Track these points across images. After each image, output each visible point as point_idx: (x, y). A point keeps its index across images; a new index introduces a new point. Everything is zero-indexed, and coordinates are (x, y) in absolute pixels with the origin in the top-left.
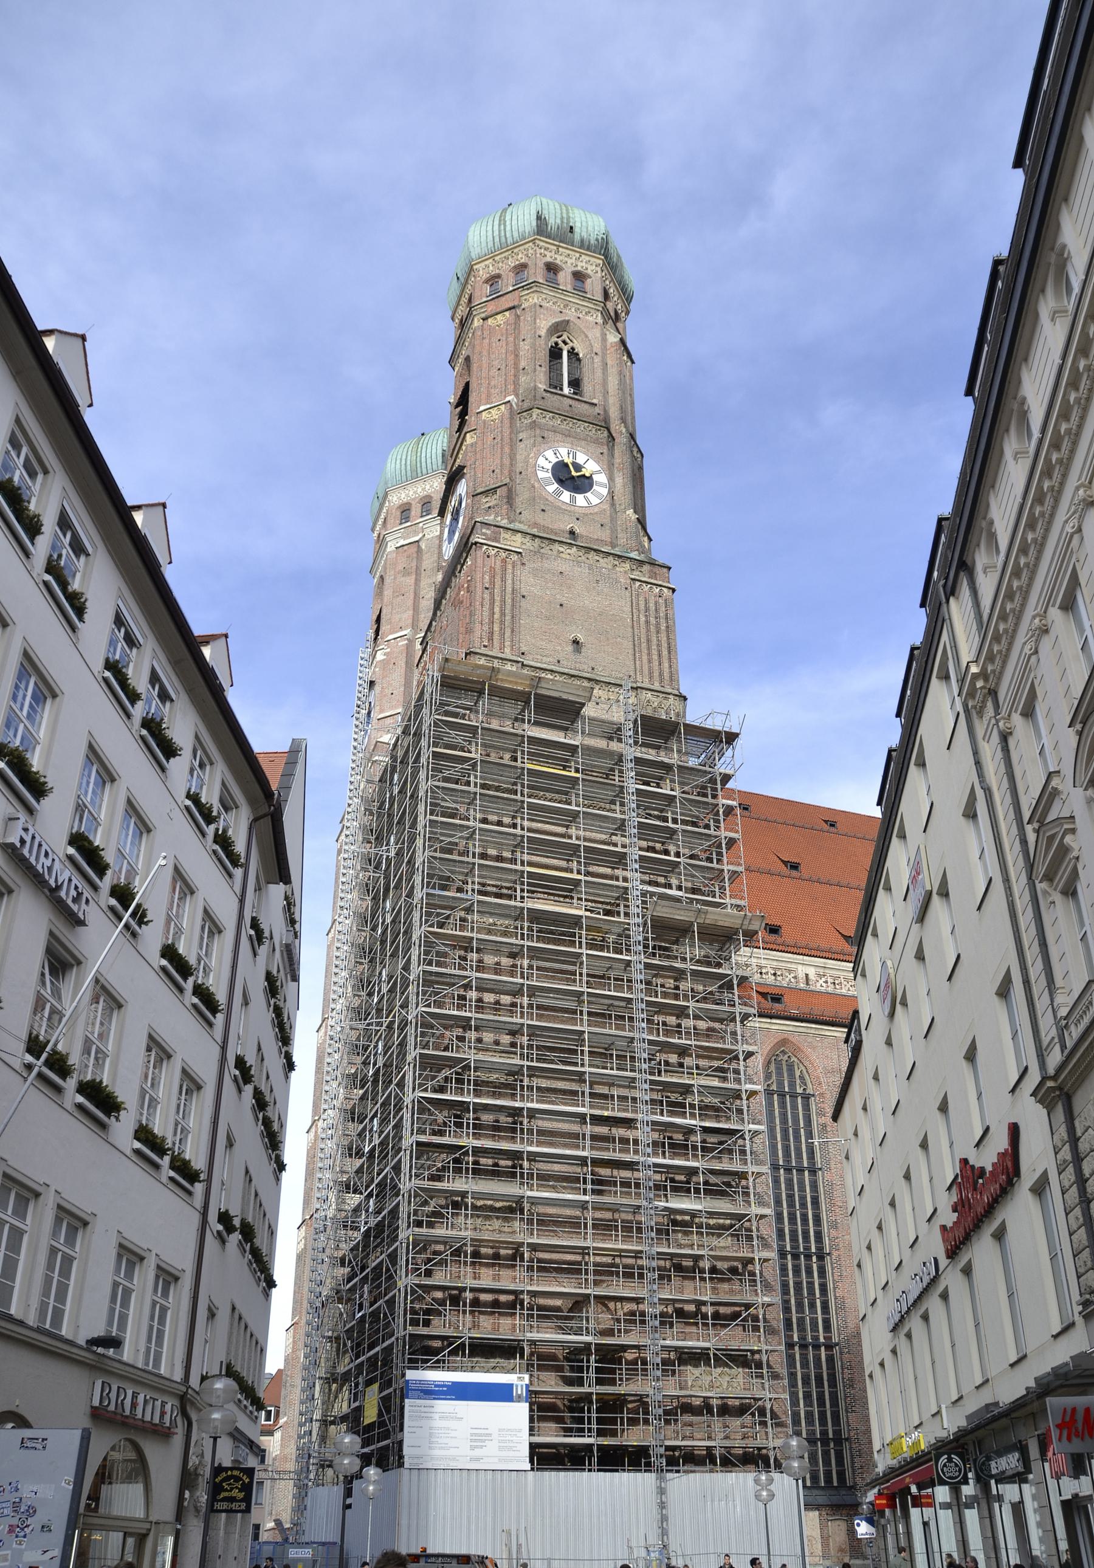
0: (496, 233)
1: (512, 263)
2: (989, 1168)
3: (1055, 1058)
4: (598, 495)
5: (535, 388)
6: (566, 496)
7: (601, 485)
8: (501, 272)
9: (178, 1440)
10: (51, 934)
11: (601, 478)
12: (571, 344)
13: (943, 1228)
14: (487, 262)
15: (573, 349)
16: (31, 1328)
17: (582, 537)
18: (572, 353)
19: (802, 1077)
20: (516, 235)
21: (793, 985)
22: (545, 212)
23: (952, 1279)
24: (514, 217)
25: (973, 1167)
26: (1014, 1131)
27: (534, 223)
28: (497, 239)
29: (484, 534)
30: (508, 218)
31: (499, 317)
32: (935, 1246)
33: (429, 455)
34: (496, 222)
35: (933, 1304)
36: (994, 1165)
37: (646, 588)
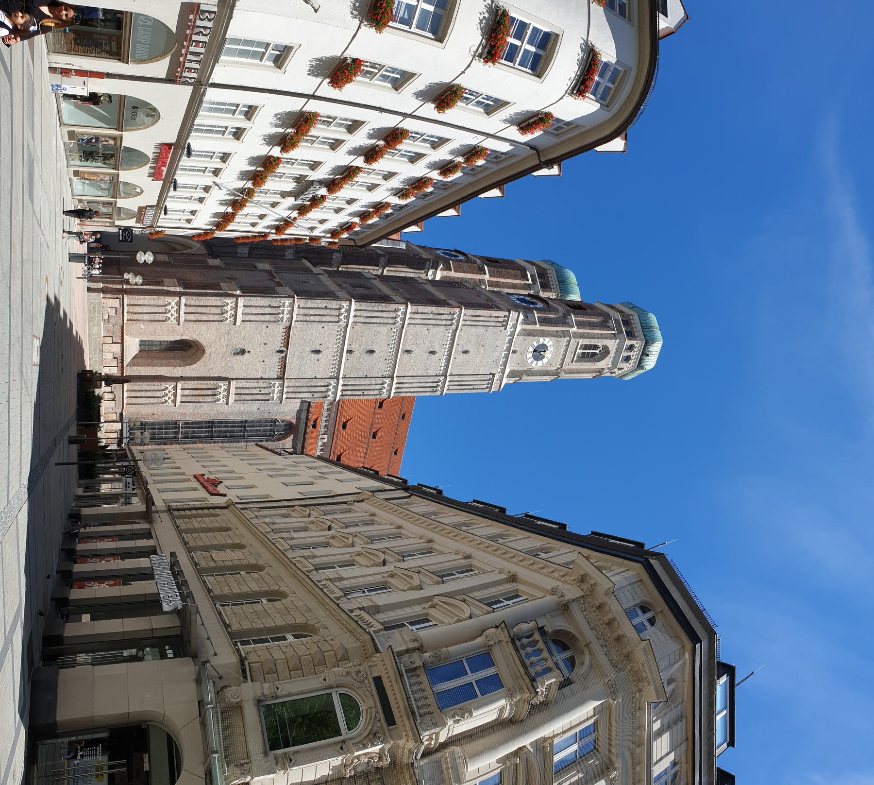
4: (532, 363)
7: (537, 364)
11: (540, 363)
25: (218, 484)
26: (225, 495)
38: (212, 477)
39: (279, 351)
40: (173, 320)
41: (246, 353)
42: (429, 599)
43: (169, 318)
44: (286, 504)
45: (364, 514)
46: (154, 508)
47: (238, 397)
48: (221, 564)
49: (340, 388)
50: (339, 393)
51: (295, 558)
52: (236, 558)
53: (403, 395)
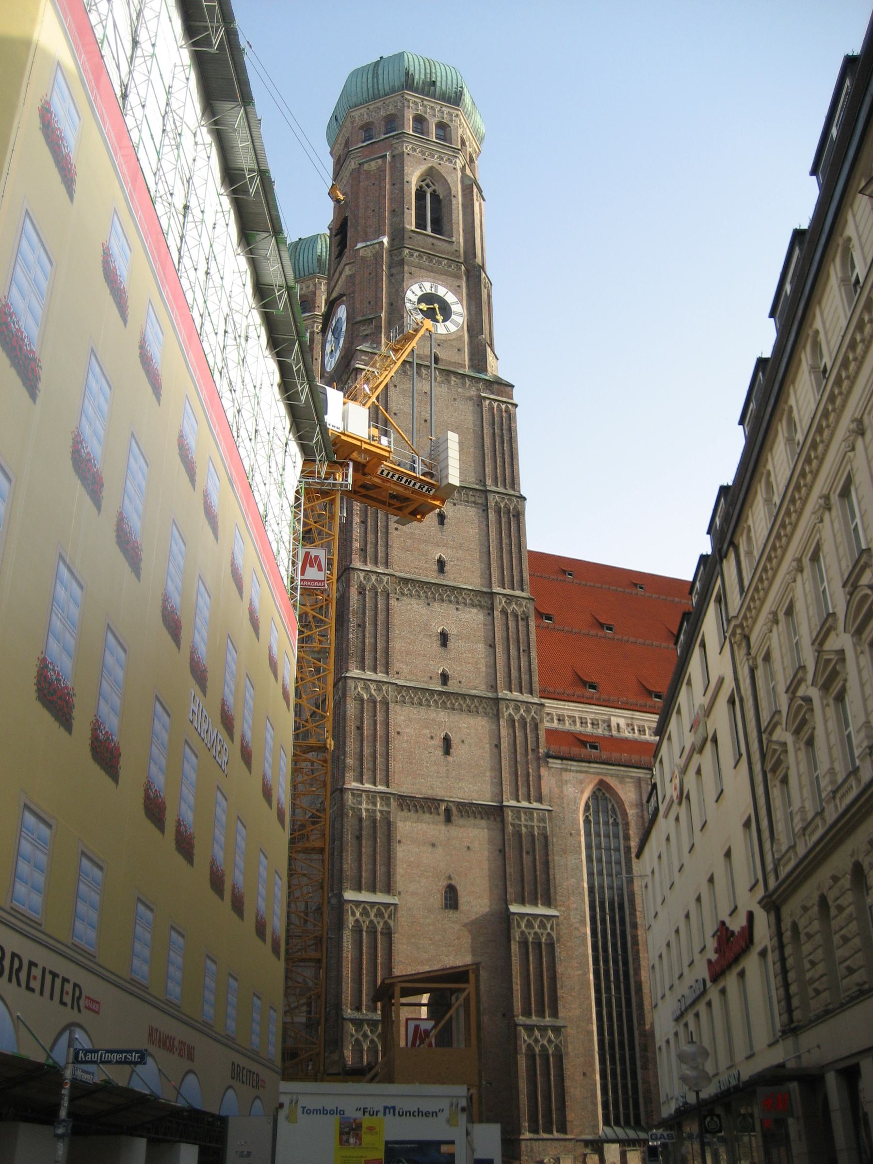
0: (370, 85)
1: (382, 113)
2: (736, 934)
3: (772, 883)
4: (455, 323)
5: (403, 228)
8: (375, 122)
12: (433, 187)
13: (709, 962)
14: (362, 111)
15: (434, 191)
17: (443, 360)
18: (434, 195)
19: (613, 808)
20: (387, 88)
21: (607, 733)
22: (412, 69)
23: (713, 994)
24: (386, 72)
25: (727, 929)
26: (750, 916)
27: (403, 79)
28: (371, 91)
29: (363, 360)
30: (380, 72)
31: (373, 163)
32: (702, 972)
33: (306, 260)
34: (370, 75)
35: (701, 1007)
36: (738, 932)
37: (495, 405)
41: (453, 882)
44: (760, 790)
49: (516, 695)
50: (526, 697)
53: (526, 575)
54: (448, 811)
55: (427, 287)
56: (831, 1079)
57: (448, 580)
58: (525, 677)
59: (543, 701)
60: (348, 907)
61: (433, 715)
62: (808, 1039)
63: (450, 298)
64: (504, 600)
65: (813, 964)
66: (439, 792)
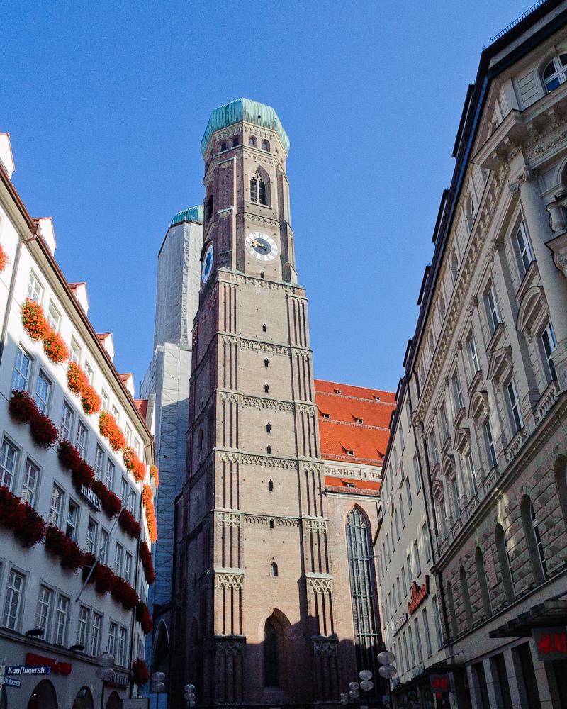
3: (437, 559)
4: (273, 255)
6: (259, 256)
7: (275, 250)
9: (128, 690)
10: (90, 517)
16: (89, 657)
25: (417, 585)
26: (427, 577)
38: (409, 593)
39: (272, 526)
40: (240, 647)
41: (275, 561)
42: (521, 337)
43: (239, 651)
45: (435, 421)
46: (449, 662)
47: (324, 569)
48: (500, 575)
51: (485, 491)
52: (492, 558)
54: (272, 524)
55: (258, 235)
56: (469, 669)
57: (270, 396)
58: (313, 448)
59: (323, 461)
60: (216, 575)
61: (263, 470)
62: (458, 648)
63: (270, 241)
64: (301, 406)
65: (458, 605)
66: (267, 512)
